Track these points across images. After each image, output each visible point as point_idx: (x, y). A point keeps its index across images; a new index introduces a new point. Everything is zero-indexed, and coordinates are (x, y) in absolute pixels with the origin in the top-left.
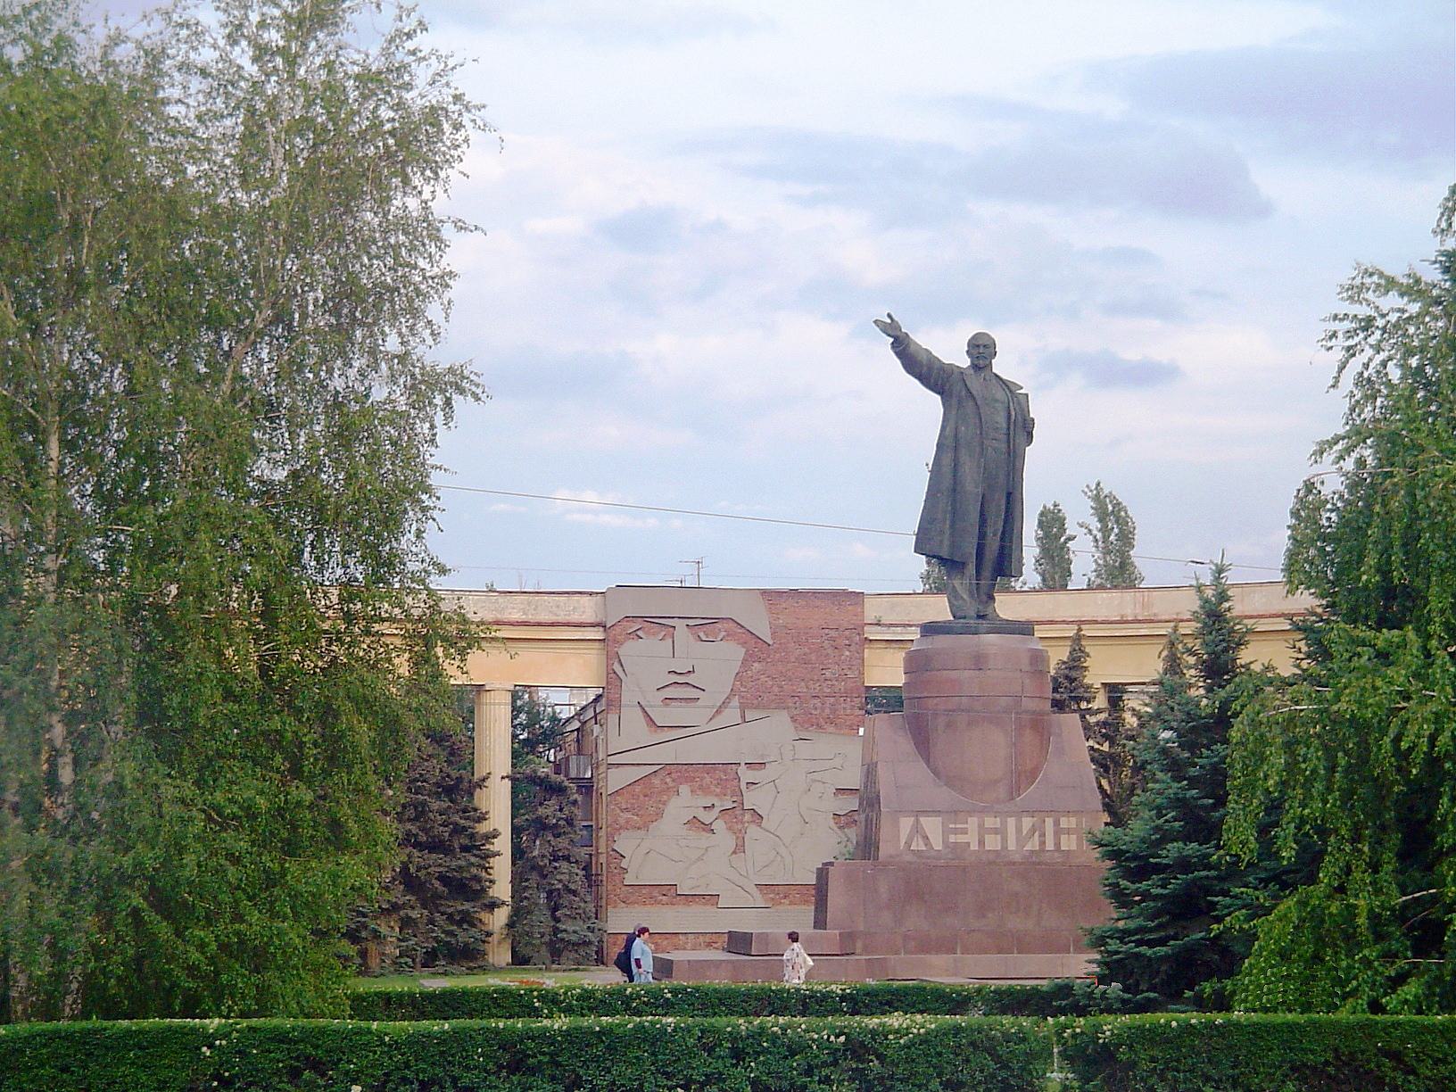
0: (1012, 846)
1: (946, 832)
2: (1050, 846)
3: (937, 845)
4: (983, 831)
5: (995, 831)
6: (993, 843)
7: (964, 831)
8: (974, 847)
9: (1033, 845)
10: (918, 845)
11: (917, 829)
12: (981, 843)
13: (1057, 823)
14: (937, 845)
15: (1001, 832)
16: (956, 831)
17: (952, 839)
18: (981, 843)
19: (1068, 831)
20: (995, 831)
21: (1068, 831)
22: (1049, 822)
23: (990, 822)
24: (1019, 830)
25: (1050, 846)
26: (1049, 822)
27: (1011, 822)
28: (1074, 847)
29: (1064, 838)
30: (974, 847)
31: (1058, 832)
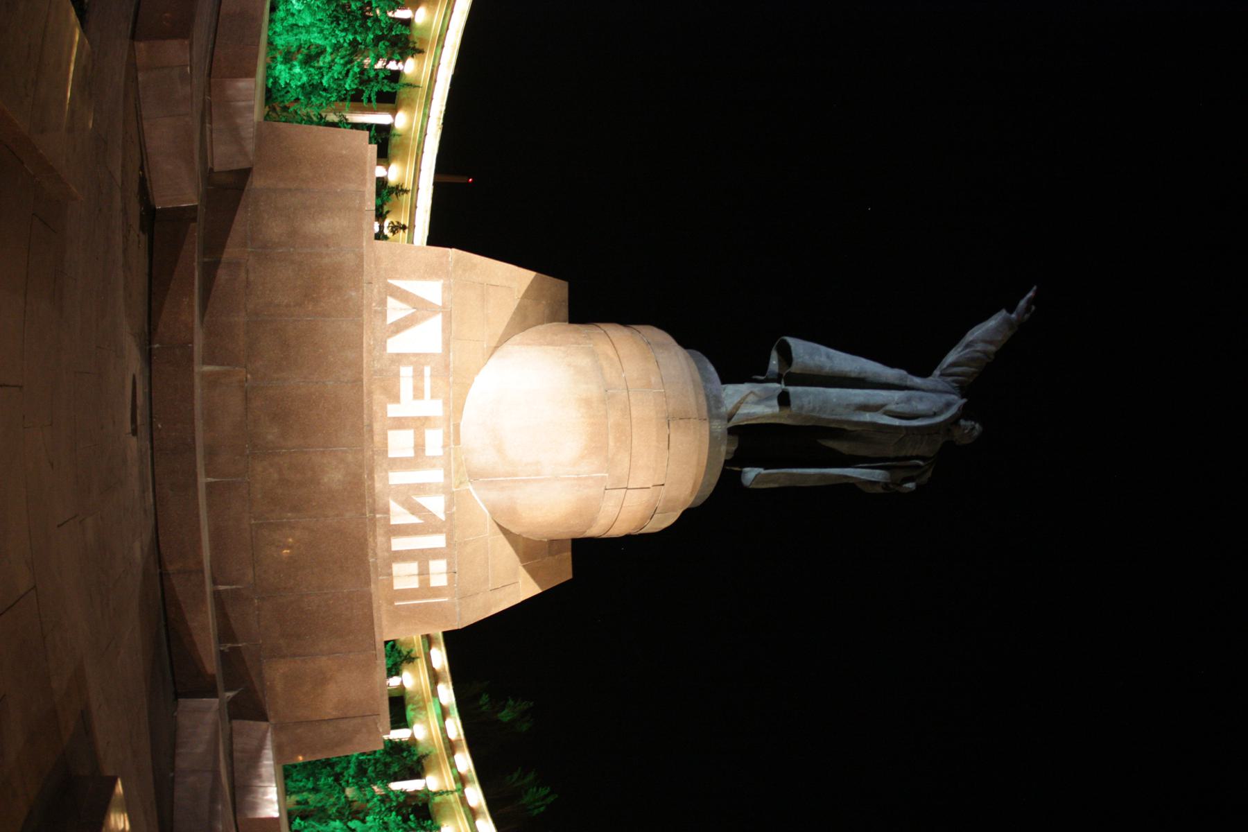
0: (397, 478)
1: (417, 360)
2: (399, 544)
3: (395, 345)
4: (419, 424)
5: (419, 447)
6: (399, 443)
7: (418, 393)
8: (393, 411)
9: (399, 515)
10: (396, 310)
11: (422, 308)
12: (400, 423)
13: (435, 554)
14: (395, 345)
15: (418, 458)
16: (418, 375)
17: (406, 372)
18: (400, 423)
19: (424, 573)
20: (419, 447)
21: (424, 573)
22: (438, 541)
23: (434, 441)
24: (421, 488)
25: (399, 544)
26: (438, 541)
27: (435, 476)
28: (399, 585)
29: (413, 567)
30: (393, 411)
31: (422, 557)
